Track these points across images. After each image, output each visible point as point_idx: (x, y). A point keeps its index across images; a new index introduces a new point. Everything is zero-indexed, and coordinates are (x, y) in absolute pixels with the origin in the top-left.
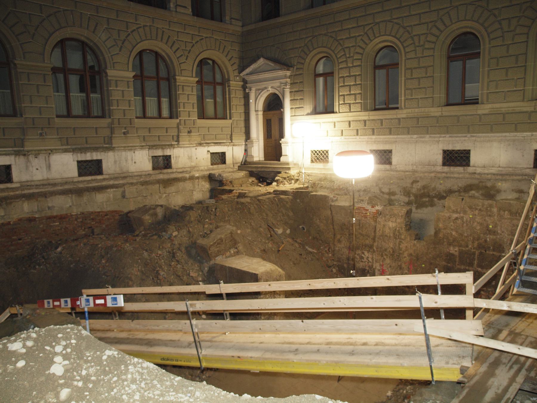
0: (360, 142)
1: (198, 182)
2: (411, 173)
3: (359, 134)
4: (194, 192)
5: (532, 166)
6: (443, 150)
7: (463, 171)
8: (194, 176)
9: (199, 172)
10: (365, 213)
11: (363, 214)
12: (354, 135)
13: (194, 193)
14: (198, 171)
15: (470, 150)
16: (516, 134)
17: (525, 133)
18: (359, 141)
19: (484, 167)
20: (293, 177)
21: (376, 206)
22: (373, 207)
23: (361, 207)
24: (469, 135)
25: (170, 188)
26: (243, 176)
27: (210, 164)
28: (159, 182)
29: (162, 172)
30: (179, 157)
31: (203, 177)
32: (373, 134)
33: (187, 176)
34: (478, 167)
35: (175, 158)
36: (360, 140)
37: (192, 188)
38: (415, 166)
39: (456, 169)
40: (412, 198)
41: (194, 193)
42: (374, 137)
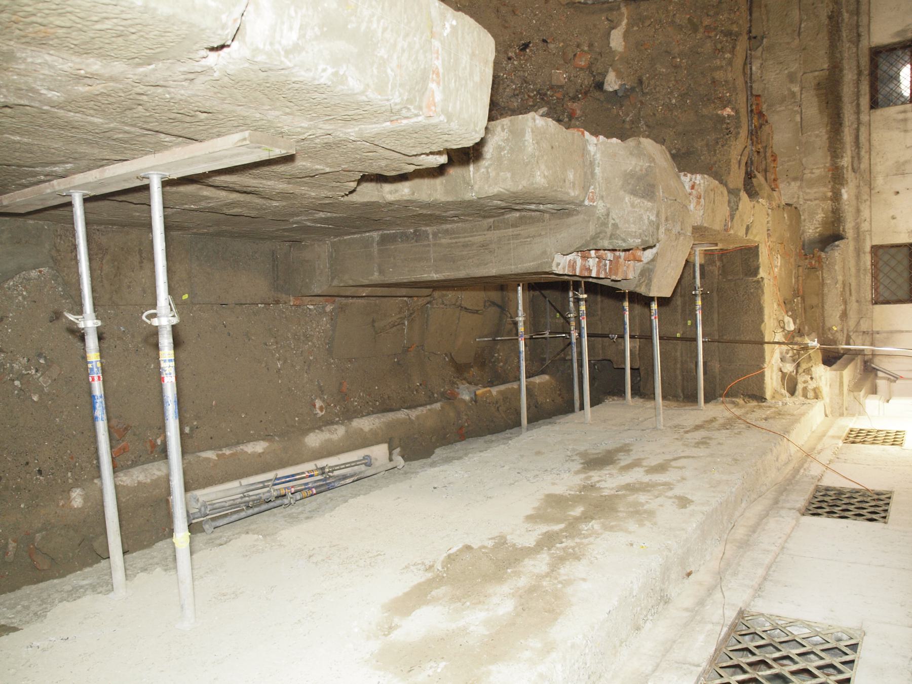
1: (825, 198)
4: (798, 184)
8: (842, 184)
9: (854, 202)
13: (795, 185)
14: (858, 197)
20: (804, 366)
25: (815, 99)
26: (830, 329)
27: (877, 241)
28: (835, 70)
29: (863, 78)
30: (906, 131)
31: (836, 217)
33: (846, 161)
35: (901, 116)
37: (808, 176)
39: (701, 638)
40: (606, 493)
41: (793, 183)
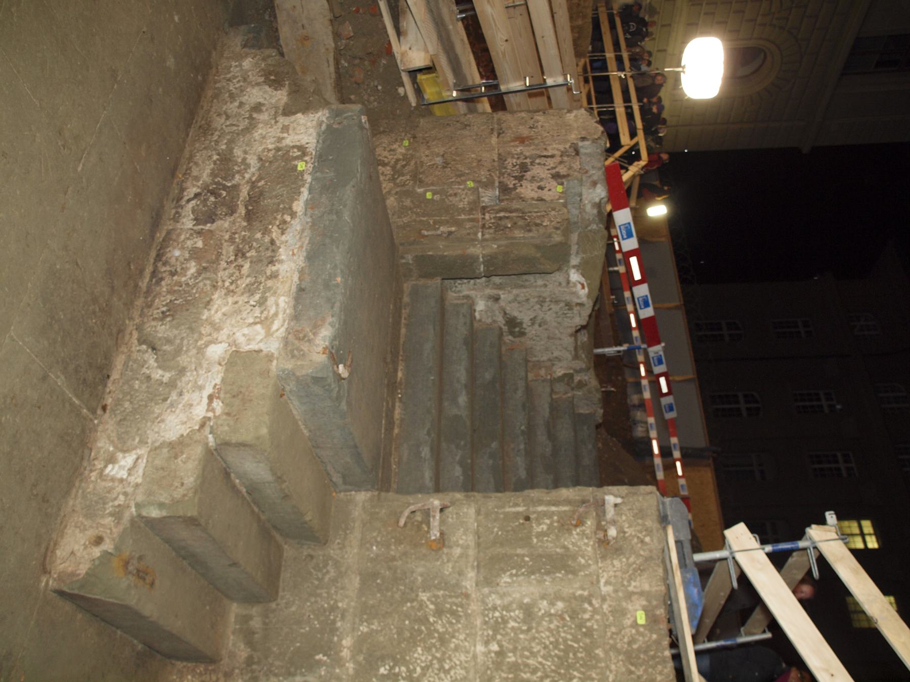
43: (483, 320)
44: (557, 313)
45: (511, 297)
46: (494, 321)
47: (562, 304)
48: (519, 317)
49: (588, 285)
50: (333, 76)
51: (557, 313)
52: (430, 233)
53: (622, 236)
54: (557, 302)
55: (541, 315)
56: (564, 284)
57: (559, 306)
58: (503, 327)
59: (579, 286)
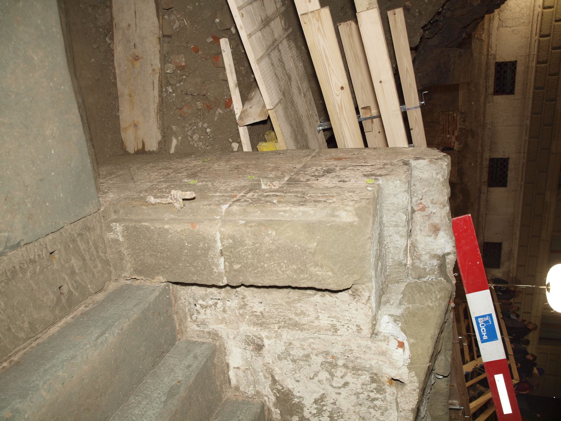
0: (530, 44)
2: (482, 123)
3: (541, 39)
5: (485, 241)
6: (508, 159)
7: (483, 181)
10: (448, 131)
11: (447, 127)
12: (540, 31)
15: (506, 186)
16: (519, 225)
17: (518, 233)
18: (531, 41)
19: (487, 201)
21: (458, 143)
22: (457, 138)
23: (456, 124)
24: (523, 183)
32: (538, 62)
34: (487, 196)
36: (533, 41)
38: (490, 126)
39: (485, 174)
42: (534, 64)
43: (242, 389)
44: (357, 394)
45: (280, 348)
46: (258, 392)
47: (366, 378)
48: (296, 393)
49: (412, 346)
50: (157, 100)
51: (357, 394)
52: (158, 200)
53: (481, 336)
54: (357, 370)
55: (332, 396)
56: (366, 331)
57: (361, 381)
58: (273, 409)
59: (394, 344)
